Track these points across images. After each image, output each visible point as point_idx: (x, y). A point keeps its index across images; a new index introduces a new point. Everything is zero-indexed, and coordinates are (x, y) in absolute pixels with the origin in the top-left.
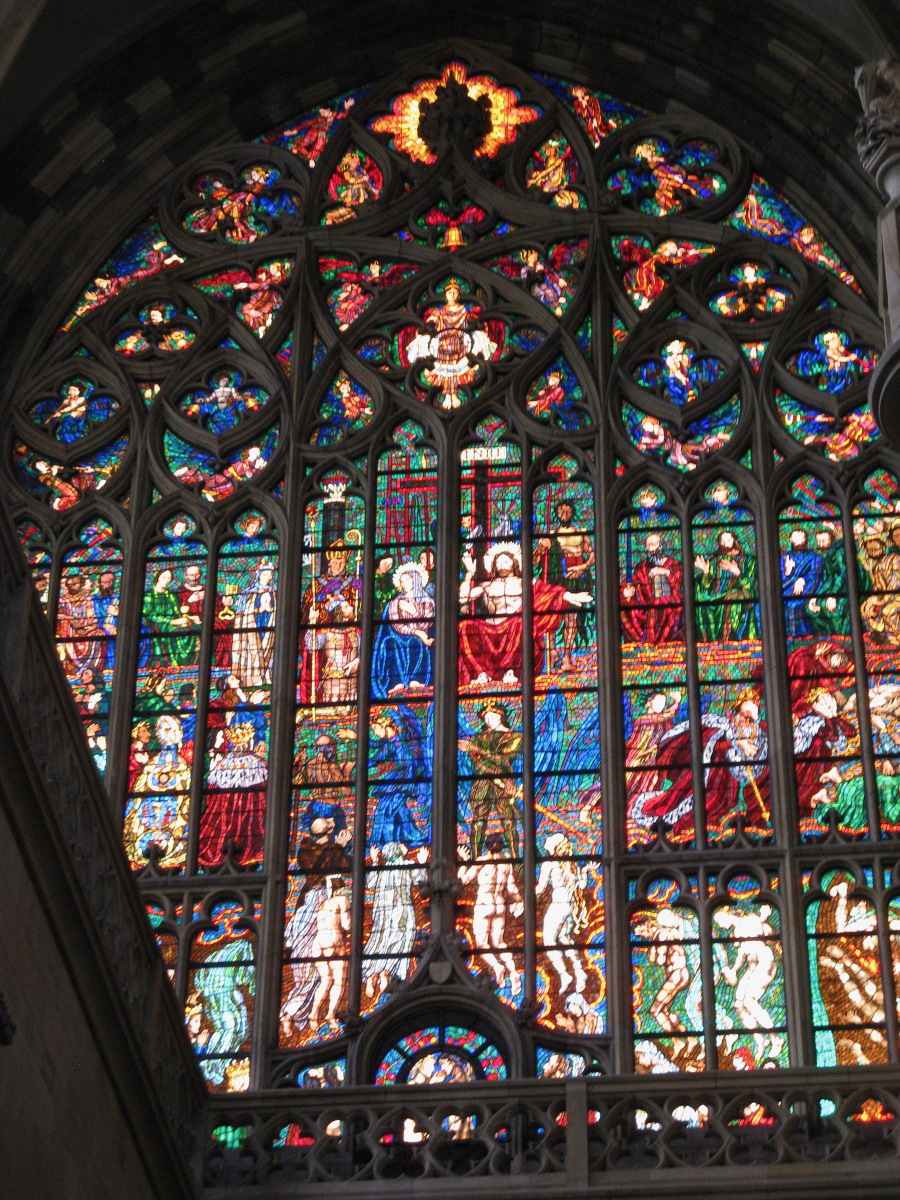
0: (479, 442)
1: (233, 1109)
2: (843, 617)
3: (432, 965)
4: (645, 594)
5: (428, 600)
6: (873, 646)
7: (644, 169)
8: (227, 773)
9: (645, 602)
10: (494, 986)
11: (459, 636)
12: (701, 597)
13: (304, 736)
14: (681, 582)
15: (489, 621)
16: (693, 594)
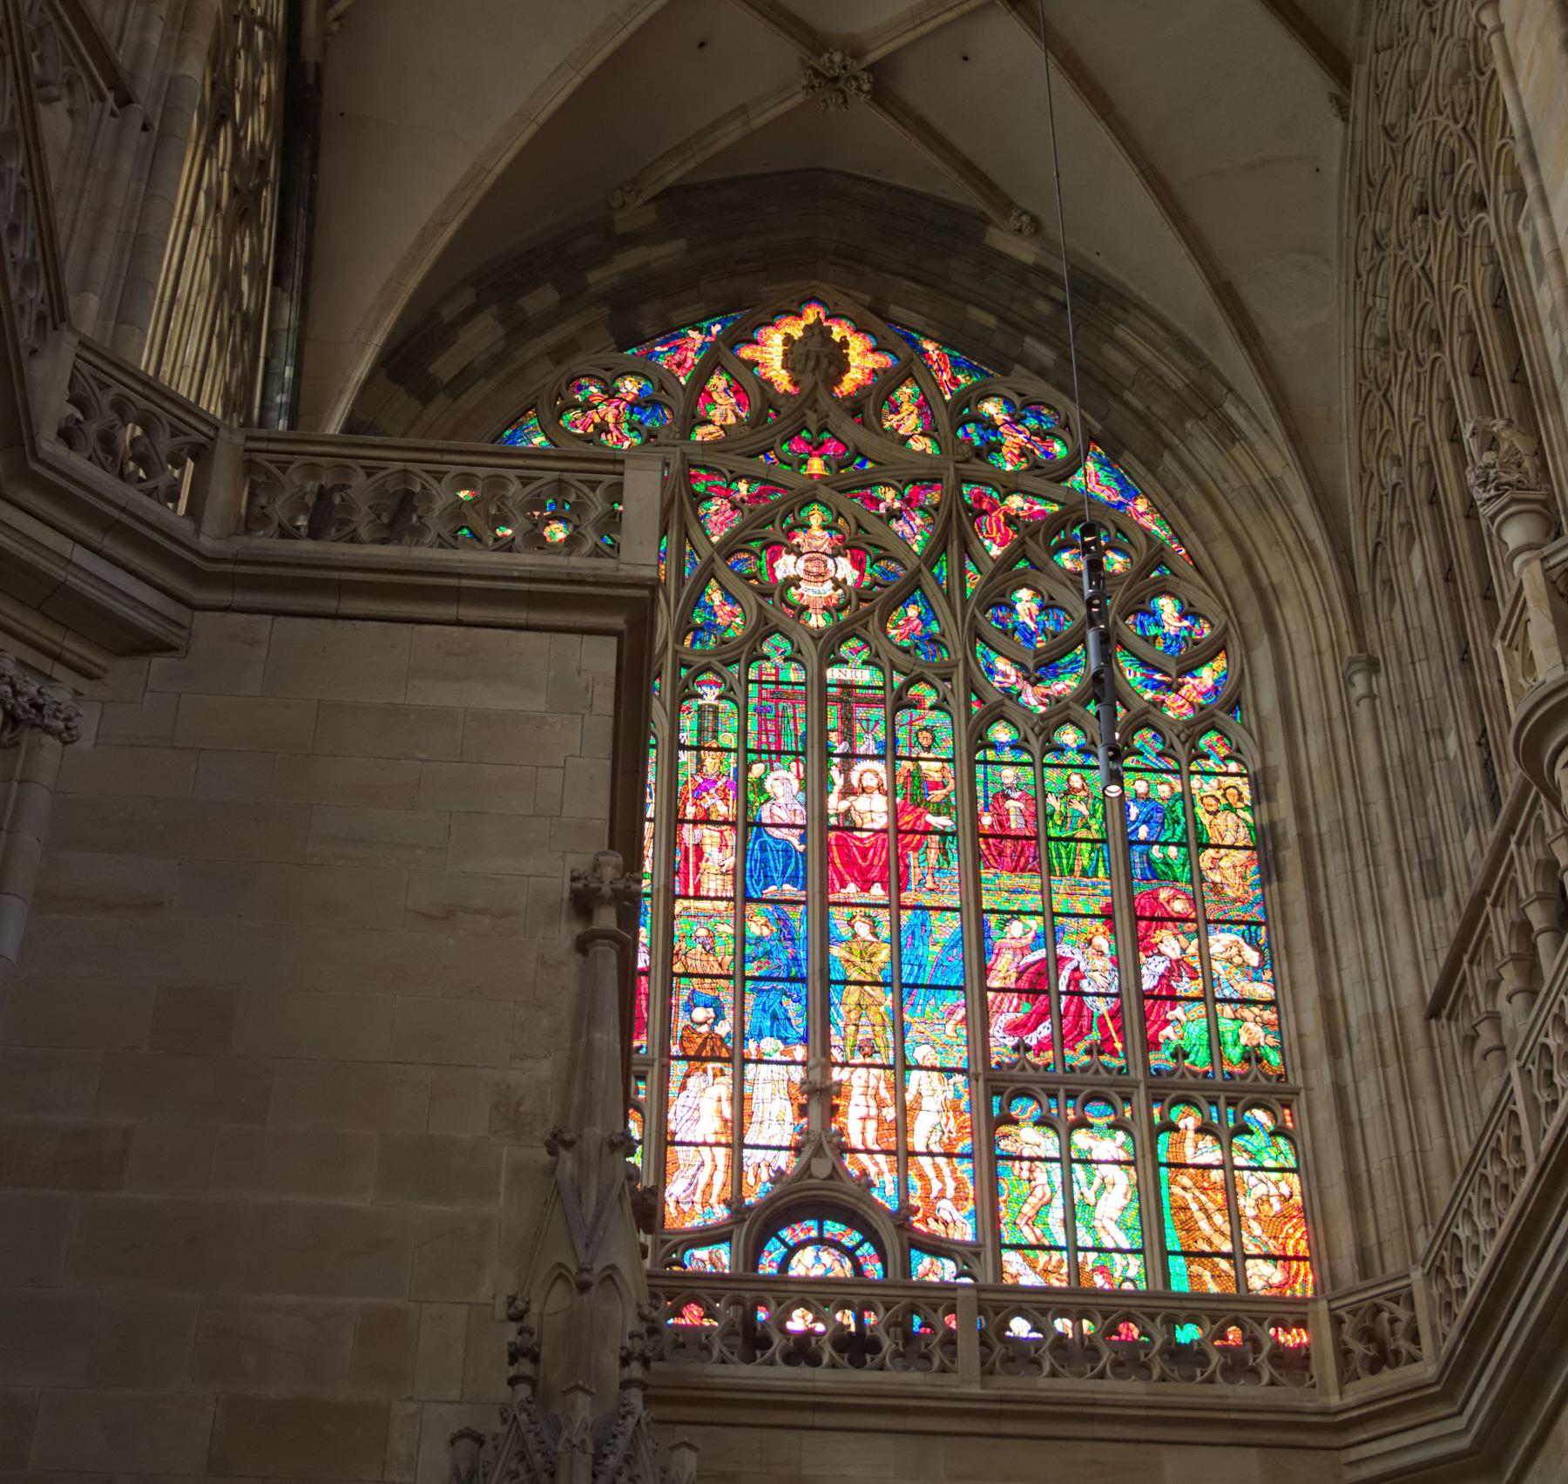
2: (1184, 865)
3: (814, 1161)
4: (1001, 824)
5: (798, 807)
7: (988, 425)
9: (1001, 833)
10: (871, 1184)
11: (829, 845)
12: (1053, 833)
13: (682, 926)
14: (1035, 815)
15: (857, 834)
16: (1046, 828)
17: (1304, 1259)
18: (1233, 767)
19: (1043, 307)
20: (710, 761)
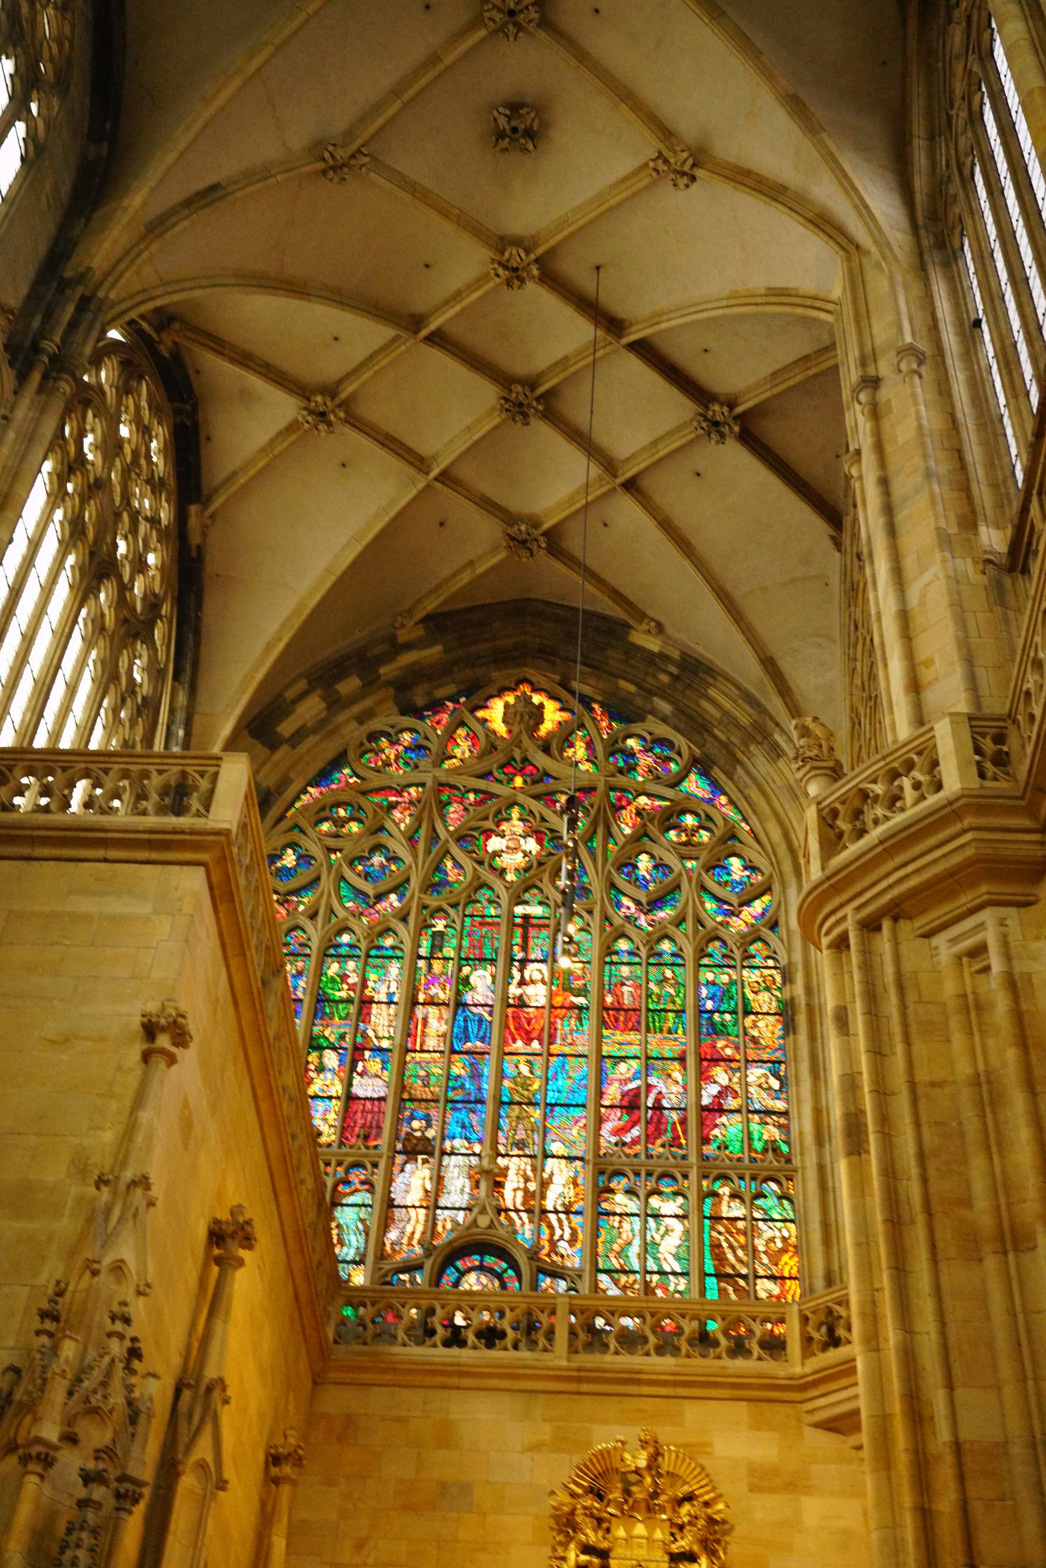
0: (526, 903)
1: (356, 1297)
6: (752, 1045)
7: (631, 754)
8: (362, 1087)
9: (618, 1008)
10: (515, 1232)
12: (651, 1006)
17: (795, 1278)
18: (771, 963)
19: (664, 678)
20: (437, 966)
